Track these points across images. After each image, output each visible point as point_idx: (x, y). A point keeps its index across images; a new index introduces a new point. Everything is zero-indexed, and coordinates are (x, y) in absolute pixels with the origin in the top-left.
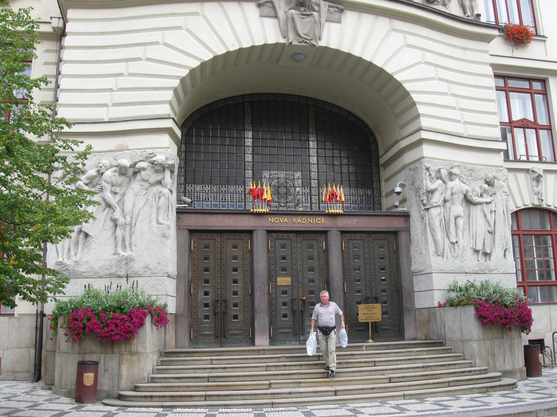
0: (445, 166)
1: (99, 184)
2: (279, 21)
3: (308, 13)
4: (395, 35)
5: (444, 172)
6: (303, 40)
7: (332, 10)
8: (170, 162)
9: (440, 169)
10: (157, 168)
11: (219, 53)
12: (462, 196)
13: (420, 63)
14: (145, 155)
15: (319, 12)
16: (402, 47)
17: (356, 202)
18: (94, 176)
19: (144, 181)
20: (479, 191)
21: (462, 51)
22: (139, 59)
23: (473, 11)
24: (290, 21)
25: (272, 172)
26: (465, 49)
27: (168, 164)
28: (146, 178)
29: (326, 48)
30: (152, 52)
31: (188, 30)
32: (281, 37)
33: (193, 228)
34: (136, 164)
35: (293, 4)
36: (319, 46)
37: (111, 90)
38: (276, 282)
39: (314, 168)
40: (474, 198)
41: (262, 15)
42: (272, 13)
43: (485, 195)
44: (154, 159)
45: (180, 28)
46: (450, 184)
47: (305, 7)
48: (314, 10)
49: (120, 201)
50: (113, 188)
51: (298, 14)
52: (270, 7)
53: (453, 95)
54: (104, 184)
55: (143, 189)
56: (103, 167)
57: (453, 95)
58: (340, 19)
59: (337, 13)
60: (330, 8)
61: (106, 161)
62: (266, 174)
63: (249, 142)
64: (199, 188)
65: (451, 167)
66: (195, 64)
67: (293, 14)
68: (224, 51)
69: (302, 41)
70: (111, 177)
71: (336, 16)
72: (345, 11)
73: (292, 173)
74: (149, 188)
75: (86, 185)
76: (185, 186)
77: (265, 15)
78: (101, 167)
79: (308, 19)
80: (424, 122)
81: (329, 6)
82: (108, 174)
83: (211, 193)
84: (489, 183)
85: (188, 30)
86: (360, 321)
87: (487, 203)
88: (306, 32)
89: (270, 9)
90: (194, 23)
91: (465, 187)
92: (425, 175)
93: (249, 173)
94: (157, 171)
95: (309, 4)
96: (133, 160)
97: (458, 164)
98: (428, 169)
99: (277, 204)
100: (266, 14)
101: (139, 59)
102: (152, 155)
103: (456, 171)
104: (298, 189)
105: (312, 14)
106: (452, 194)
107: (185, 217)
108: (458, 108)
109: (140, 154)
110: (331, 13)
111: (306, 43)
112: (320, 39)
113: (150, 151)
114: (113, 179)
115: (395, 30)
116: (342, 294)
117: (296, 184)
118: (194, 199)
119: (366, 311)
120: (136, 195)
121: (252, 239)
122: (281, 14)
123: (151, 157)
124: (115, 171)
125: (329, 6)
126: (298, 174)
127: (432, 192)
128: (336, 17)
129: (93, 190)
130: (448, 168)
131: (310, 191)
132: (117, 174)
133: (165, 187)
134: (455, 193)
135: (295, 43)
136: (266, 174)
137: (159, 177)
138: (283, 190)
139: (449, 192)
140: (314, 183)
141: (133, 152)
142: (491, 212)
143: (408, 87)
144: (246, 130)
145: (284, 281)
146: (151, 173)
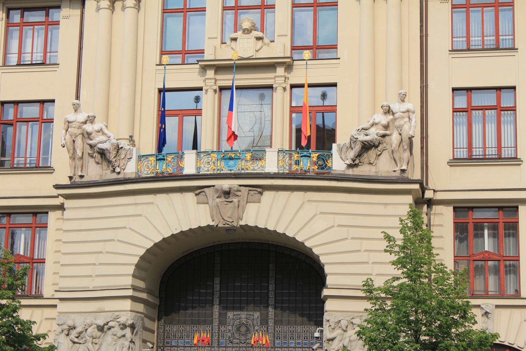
0: (345, 317)
1: (85, 337)
8: (130, 322)
9: (340, 320)
10: (122, 327)
14: (114, 316)
16: (316, 215)
17: (307, 338)
18: (81, 331)
19: (115, 335)
21: (382, 207)
22: (113, 240)
25: (235, 313)
27: (128, 324)
28: (115, 334)
30: (121, 235)
32: (211, 220)
34: (108, 322)
37: (94, 264)
41: (198, 202)
49: (98, 349)
50: (94, 340)
51: (222, 202)
53: (366, 251)
54: (88, 338)
55: (114, 341)
56: (87, 325)
57: (366, 251)
59: (257, 195)
60: (250, 192)
61: (89, 319)
62: (230, 314)
63: (217, 287)
64: (175, 328)
65: (352, 317)
67: (217, 203)
69: (224, 223)
70: (92, 333)
72: (264, 193)
73: (251, 313)
74: (117, 340)
75: (77, 337)
76: (165, 327)
77: (201, 202)
78: (85, 325)
79: (230, 205)
80: (329, 281)
82: (90, 330)
83: (185, 332)
88: (229, 215)
89: (204, 197)
94: (122, 329)
96: (106, 320)
99: (238, 341)
100: (201, 201)
101: (113, 240)
102: (118, 317)
104: (256, 328)
106: (350, 340)
108: (370, 262)
109: (110, 316)
110: (252, 195)
111: (228, 224)
113: (117, 314)
114: (94, 334)
117: (255, 322)
118: (171, 337)
120: (109, 345)
122: (210, 201)
123: (118, 318)
124: (94, 328)
125: (249, 190)
126: (257, 314)
127: (332, 340)
129: (81, 341)
130: (350, 319)
131: (268, 329)
132: (96, 330)
133: (127, 340)
135: (220, 225)
138: (243, 329)
140: (271, 323)
141: (106, 314)
143: (316, 251)
144: (216, 277)
146: (117, 329)
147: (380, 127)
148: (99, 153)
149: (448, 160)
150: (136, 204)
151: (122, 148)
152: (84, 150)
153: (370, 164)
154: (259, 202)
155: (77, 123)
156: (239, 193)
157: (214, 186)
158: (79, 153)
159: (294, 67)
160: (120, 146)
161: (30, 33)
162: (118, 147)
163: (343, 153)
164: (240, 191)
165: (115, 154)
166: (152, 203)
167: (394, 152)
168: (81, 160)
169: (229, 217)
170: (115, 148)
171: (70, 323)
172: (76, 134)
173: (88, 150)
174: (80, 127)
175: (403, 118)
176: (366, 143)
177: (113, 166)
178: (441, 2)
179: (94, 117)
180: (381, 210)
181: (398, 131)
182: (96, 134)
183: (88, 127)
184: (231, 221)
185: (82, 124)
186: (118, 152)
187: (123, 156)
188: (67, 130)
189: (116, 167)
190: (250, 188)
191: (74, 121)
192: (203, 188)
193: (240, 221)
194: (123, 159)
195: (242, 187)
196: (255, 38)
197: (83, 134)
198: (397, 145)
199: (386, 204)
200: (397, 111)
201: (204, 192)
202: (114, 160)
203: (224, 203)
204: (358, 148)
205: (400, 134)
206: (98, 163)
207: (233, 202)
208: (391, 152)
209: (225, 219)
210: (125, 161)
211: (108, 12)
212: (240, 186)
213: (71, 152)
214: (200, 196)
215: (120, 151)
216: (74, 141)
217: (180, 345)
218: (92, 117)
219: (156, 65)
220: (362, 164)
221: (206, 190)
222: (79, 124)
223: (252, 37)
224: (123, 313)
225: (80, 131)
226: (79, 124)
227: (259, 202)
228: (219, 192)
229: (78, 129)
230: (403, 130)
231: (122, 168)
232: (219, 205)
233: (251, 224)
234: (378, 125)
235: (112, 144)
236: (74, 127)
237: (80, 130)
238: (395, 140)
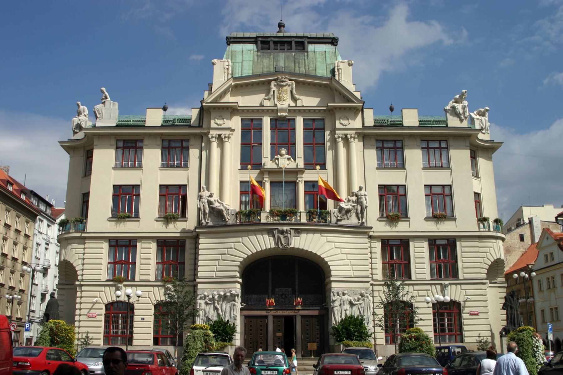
5: (340, 293)
12: (348, 302)
15: (290, 234)
20: (356, 299)
25: (280, 289)
29: (293, 247)
33: (246, 315)
38: (276, 335)
39: (297, 287)
40: (354, 302)
43: (360, 301)
44: (232, 292)
46: (343, 297)
48: (288, 233)
62: (277, 290)
66: (246, 256)
71: (297, 234)
80: (333, 273)
84: (362, 295)
86: (309, 349)
87: (360, 304)
90: (246, 239)
91: (350, 298)
92: (332, 294)
93: (270, 290)
97: (347, 289)
98: (333, 292)
103: (346, 292)
104: (290, 296)
106: (343, 301)
107: (243, 311)
112: (291, 244)
113: (230, 289)
116: (300, 339)
119: (310, 346)
121: (267, 319)
122: (276, 236)
126: (290, 289)
127: (335, 301)
134: (345, 301)
136: (277, 290)
137: (233, 299)
139: (342, 301)
142: (362, 307)
143: (326, 259)
145: (279, 334)
147: (351, 202)
149: (377, 218)
153: (348, 219)
157: (277, 228)
159: (305, 173)
161: (174, 151)
169: (285, 244)
171: (206, 293)
183: (210, 199)
188: (200, 200)
197: (208, 202)
202: (225, 215)
206: (216, 216)
212: (290, 229)
217: (253, 304)
224: (233, 289)
233: (296, 246)
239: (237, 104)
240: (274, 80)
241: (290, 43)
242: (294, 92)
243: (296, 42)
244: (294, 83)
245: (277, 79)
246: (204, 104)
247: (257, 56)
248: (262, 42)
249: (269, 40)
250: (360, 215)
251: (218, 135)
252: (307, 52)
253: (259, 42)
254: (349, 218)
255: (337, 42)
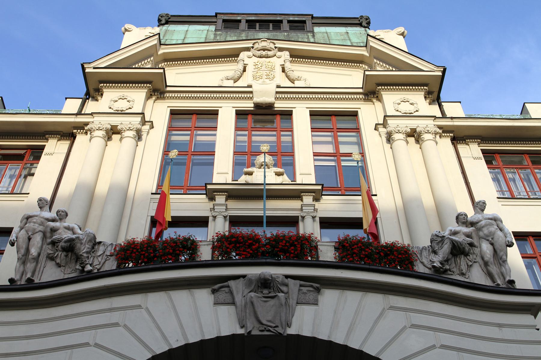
2: (236, 307)
3: (272, 294)
4: (391, 314)
6: (265, 328)
7: (304, 289)
11: (158, 352)
13: (433, 347)
23: (504, 279)
24: (249, 305)
26: (500, 326)
29: (298, 338)
31: (125, 326)
32: (238, 326)
35: (253, 287)
36: (287, 334)
41: (217, 302)
42: (228, 298)
45: (116, 325)
47: (270, 289)
51: (259, 297)
52: (226, 292)
58: (317, 300)
59: (312, 293)
67: (252, 297)
68: (166, 348)
69: (263, 329)
71: (311, 296)
77: (221, 302)
79: (272, 302)
81: (301, 286)
85: (125, 326)
88: (270, 318)
95: (274, 284)
105: (277, 295)
110: (305, 293)
112: (289, 326)
115: (392, 308)
122: (239, 299)
125: (301, 286)
128: (311, 297)
135: (255, 332)
148: (64, 249)
150: (111, 310)
151: (100, 243)
152: (43, 251)
153: (463, 274)
154: (316, 303)
155: (40, 219)
156: (284, 289)
157: (244, 276)
158: (34, 251)
160: (98, 240)
162: (95, 241)
163: (423, 257)
164: (287, 285)
165: (88, 248)
166: (139, 307)
167: (489, 264)
168: (34, 262)
170: (90, 241)
172: (34, 229)
173: (48, 249)
174: (42, 224)
175: (491, 225)
176: (456, 244)
177: (81, 264)
178: (474, 158)
179: (65, 213)
180: (494, 332)
181: (488, 240)
182: (64, 231)
184: (274, 325)
185: (46, 221)
186: (93, 248)
187: (100, 253)
189: (87, 264)
190: (302, 282)
191: (36, 216)
192: (227, 282)
193: (288, 328)
194: (100, 256)
195: (289, 279)
196: (274, 173)
198: (491, 257)
199: (500, 326)
200: (481, 218)
201: (228, 287)
202: (85, 255)
203: (261, 299)
204: (446, 248)
205: (492, 244)
207: (276, 299)
208: (483, 266)
209: (264, 322)
210: (102, 259)
211: (102, 141)
212: (287, 277)
213: (23, 251)
214: (218, 294)
215: (96, 247)
216: (29, 239)
218: (62, 211)
219: (152, 194)
220: (451, 273)
221: (232, 283)
222: (42, 219)
223: (271, 171)
225: (41, 228)
226: (42, 219)
227: (316, 303)
228: (254, 284)
229: (40, 225)
230: (495, 239)
231: (96, 267)
232: (255, 300)
233: (306, 332)
234: (458, 234)
235: (88, 235)
236: (34, 223)
237: (41, 227)
238: (487, 250)
239: (162, 71)
240: (248, 49)
241: (281, 22)
242: (288, 66)
243: (289, 22)
244: (287, 53)
245: (253, 47)
246: (87, 70)
247: (215, 34)
248: (224, 21)
249: (239, 18)
250: (494, 269)
251: (111, 125)
252: (313, 32)
253: (220, 22)
254: (464, 271)
255: (369, 23)
